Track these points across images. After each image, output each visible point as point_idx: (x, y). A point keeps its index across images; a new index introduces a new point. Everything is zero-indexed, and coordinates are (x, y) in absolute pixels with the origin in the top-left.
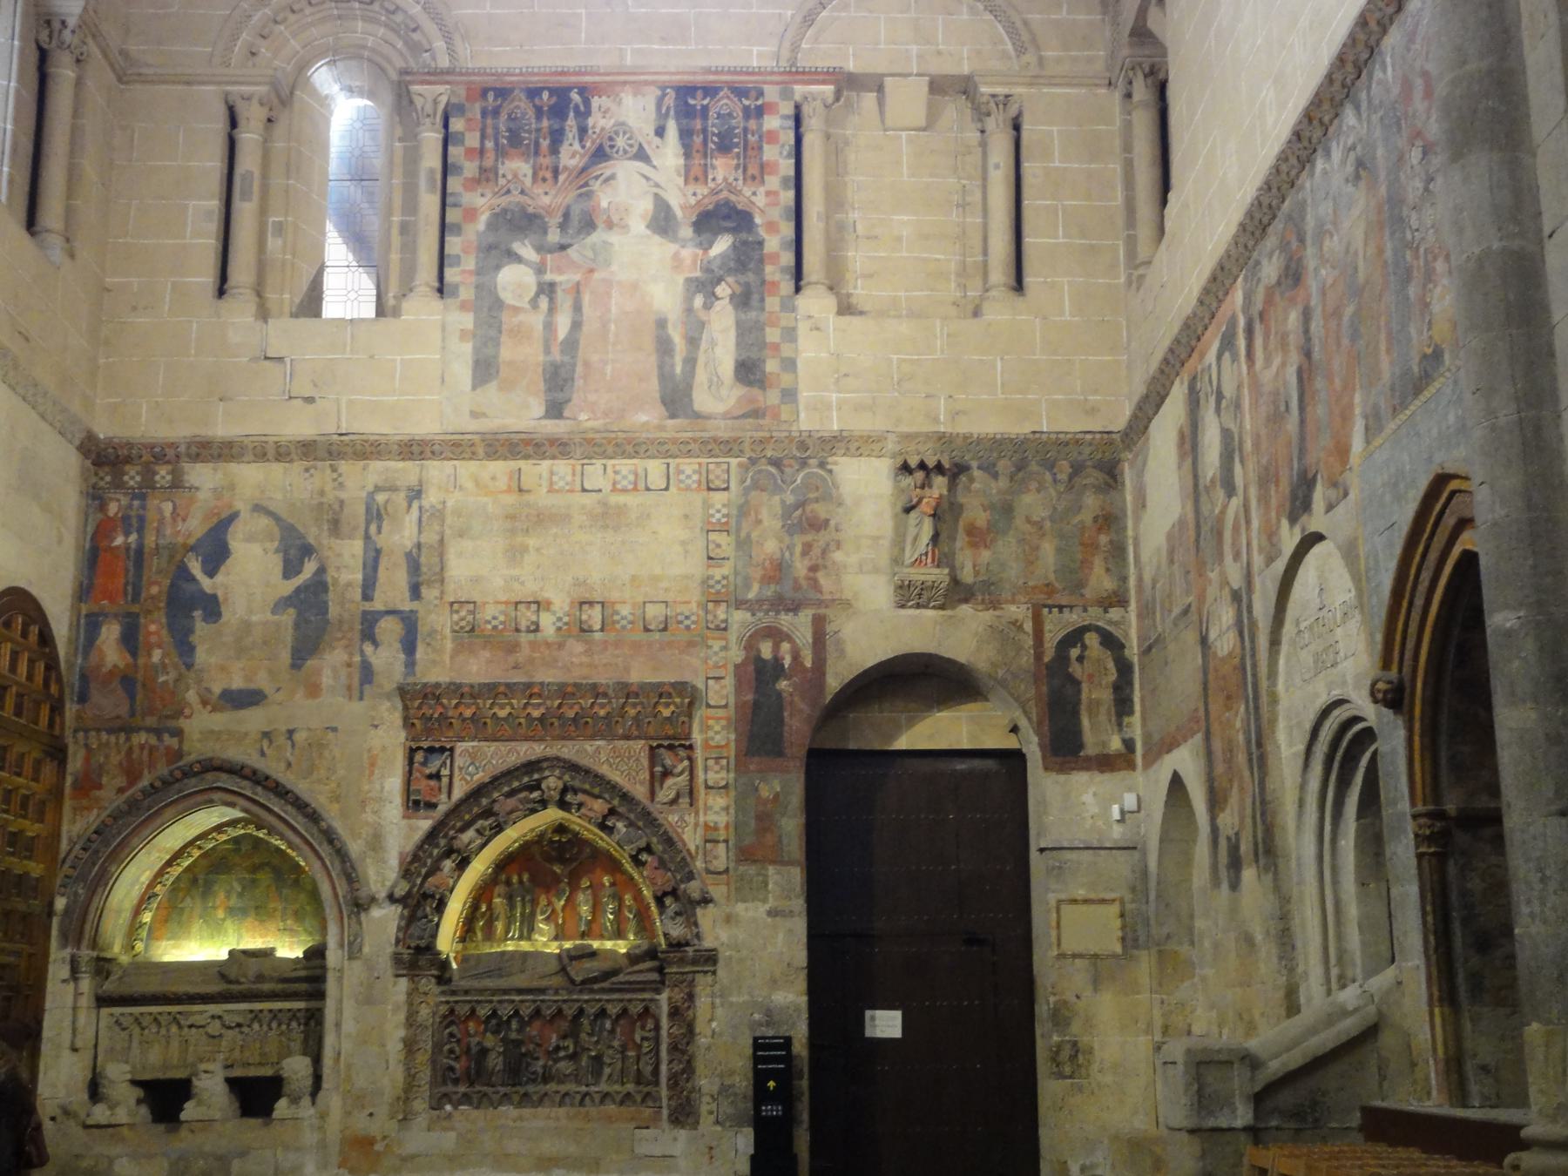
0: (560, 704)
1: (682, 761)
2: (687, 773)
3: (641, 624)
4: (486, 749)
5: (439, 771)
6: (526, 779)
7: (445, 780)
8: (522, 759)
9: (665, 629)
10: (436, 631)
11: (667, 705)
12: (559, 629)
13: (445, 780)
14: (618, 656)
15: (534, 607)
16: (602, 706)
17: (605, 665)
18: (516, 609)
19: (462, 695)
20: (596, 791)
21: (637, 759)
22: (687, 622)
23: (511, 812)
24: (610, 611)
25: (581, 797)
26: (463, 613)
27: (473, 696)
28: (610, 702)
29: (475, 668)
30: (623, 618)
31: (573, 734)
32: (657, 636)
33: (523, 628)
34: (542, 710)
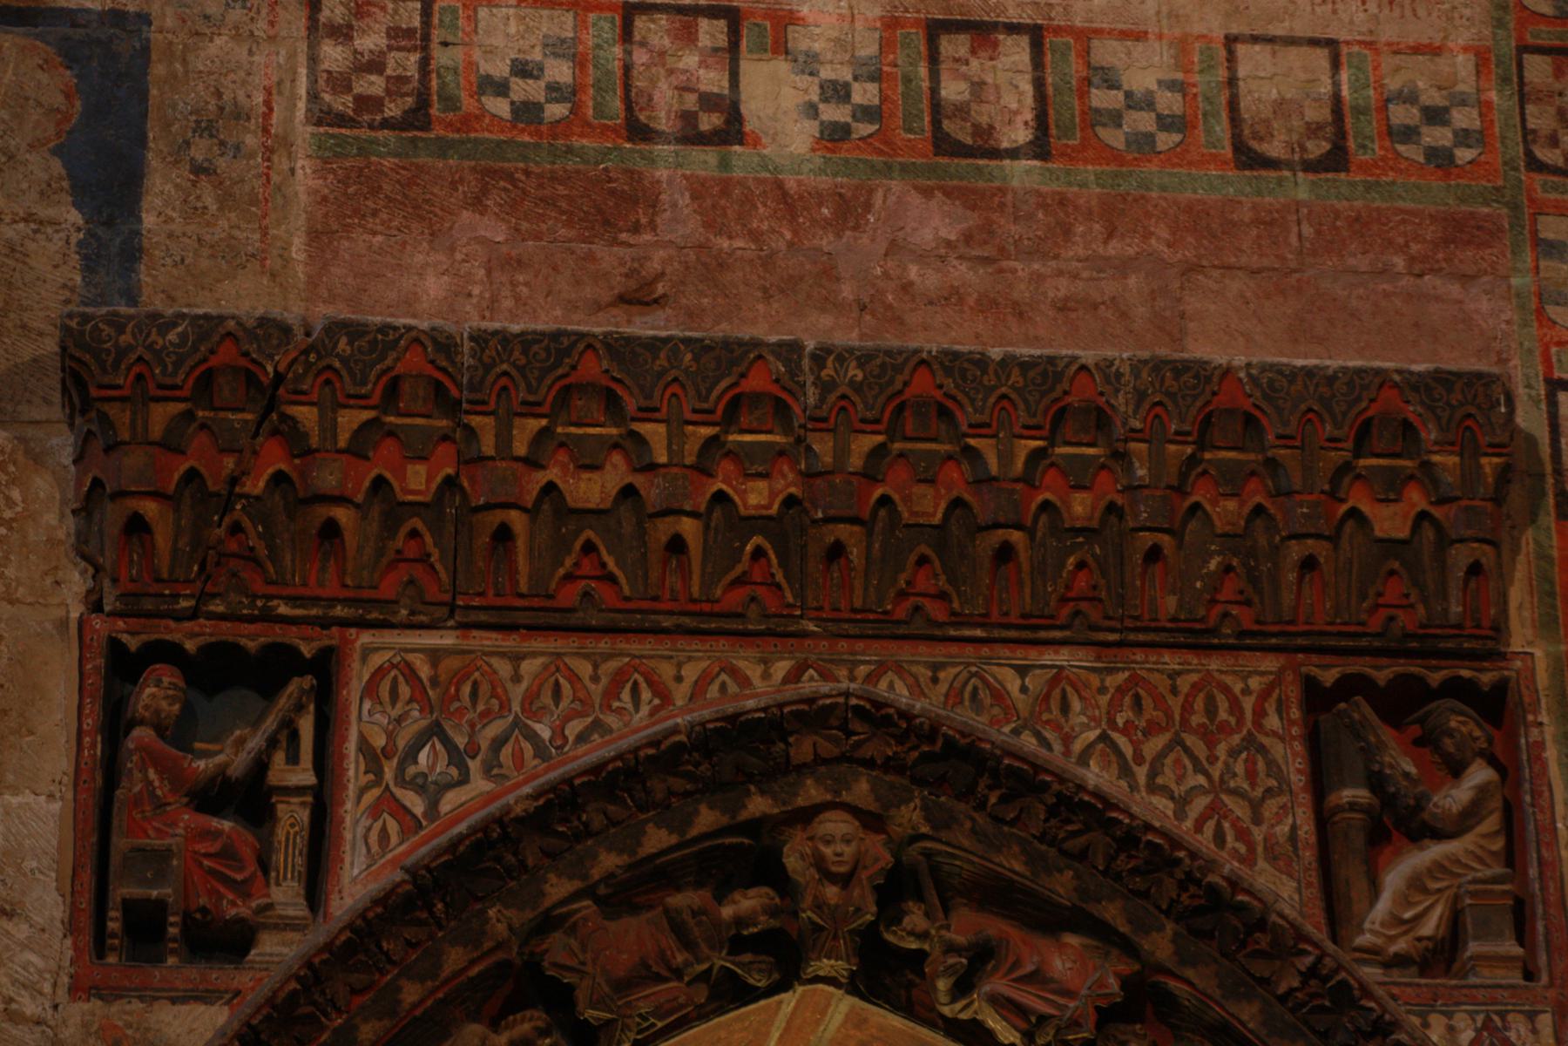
0: (878, 452)
1: (1456, 770)
2: (1491, 823)
3: (1222, 129)
4: (503, 668)
5: (261, 766)
6: (707, 818)
7: (292, 817)
8: (682, 717)
9: (1337, 159)
10: (240, 115)
11: (1391, 487)
12: (835, 135)
13: (292, 817)
14: (1123, 267)
15: (711, 32)
16: (1079, 476)
17: (1063, 307)
18: (626, 35)
19: (393, 389)
20: (1061, 886)
21: (1249, 740)
22: (1438, 136)
23: (644, 975)
24: (1075, 67)
25: (966, 925)
26: (370, 41)
27: (439, 395)
28: (1120, 456)
29: (434, 287)
30: (1134, 102)
31: (935, 610)
32: (1302, 188)
33: (664, 122)
34: (787, 482)
